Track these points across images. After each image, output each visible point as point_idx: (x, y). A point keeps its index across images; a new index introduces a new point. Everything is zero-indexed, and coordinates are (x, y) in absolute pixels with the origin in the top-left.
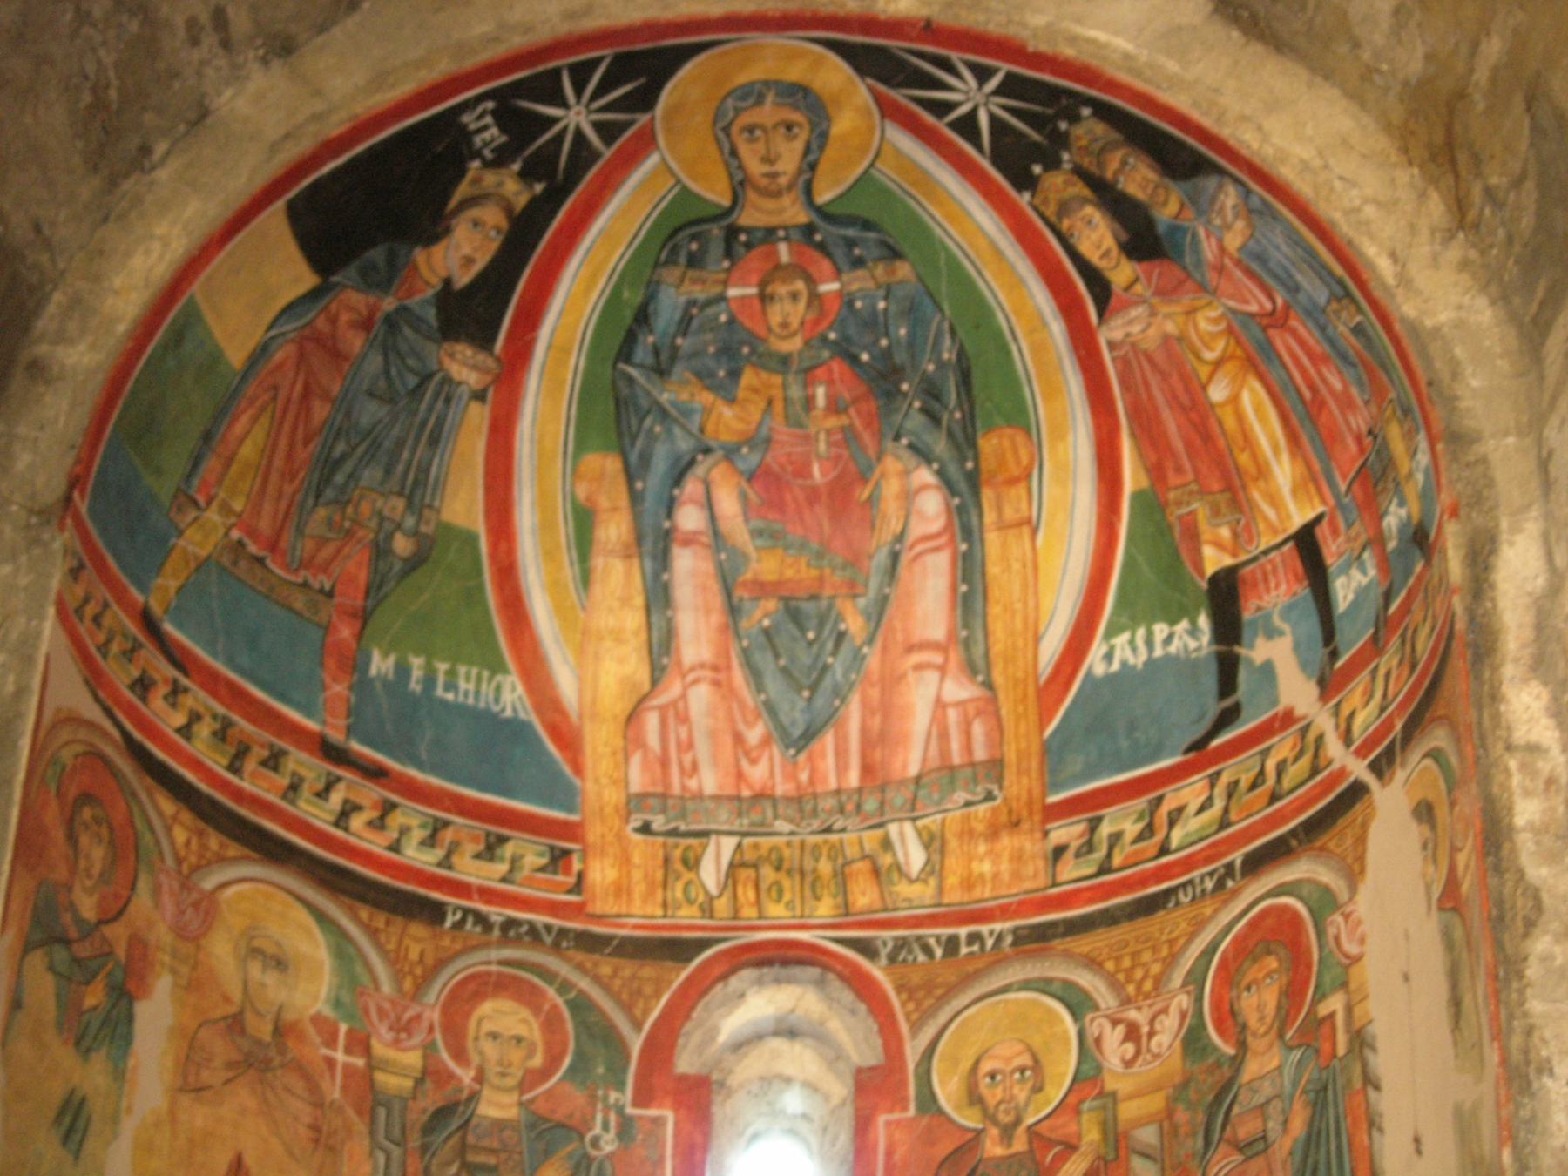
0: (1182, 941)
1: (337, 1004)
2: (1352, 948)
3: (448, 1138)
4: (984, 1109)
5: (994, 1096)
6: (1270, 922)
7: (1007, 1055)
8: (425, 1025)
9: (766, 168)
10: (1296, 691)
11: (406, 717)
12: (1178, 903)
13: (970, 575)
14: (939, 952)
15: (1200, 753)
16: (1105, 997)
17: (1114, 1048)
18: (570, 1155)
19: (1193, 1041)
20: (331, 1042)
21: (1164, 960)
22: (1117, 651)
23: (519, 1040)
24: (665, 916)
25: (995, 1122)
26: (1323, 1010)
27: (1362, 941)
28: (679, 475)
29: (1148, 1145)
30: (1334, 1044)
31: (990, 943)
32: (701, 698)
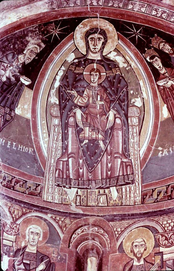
9: (94, 47)
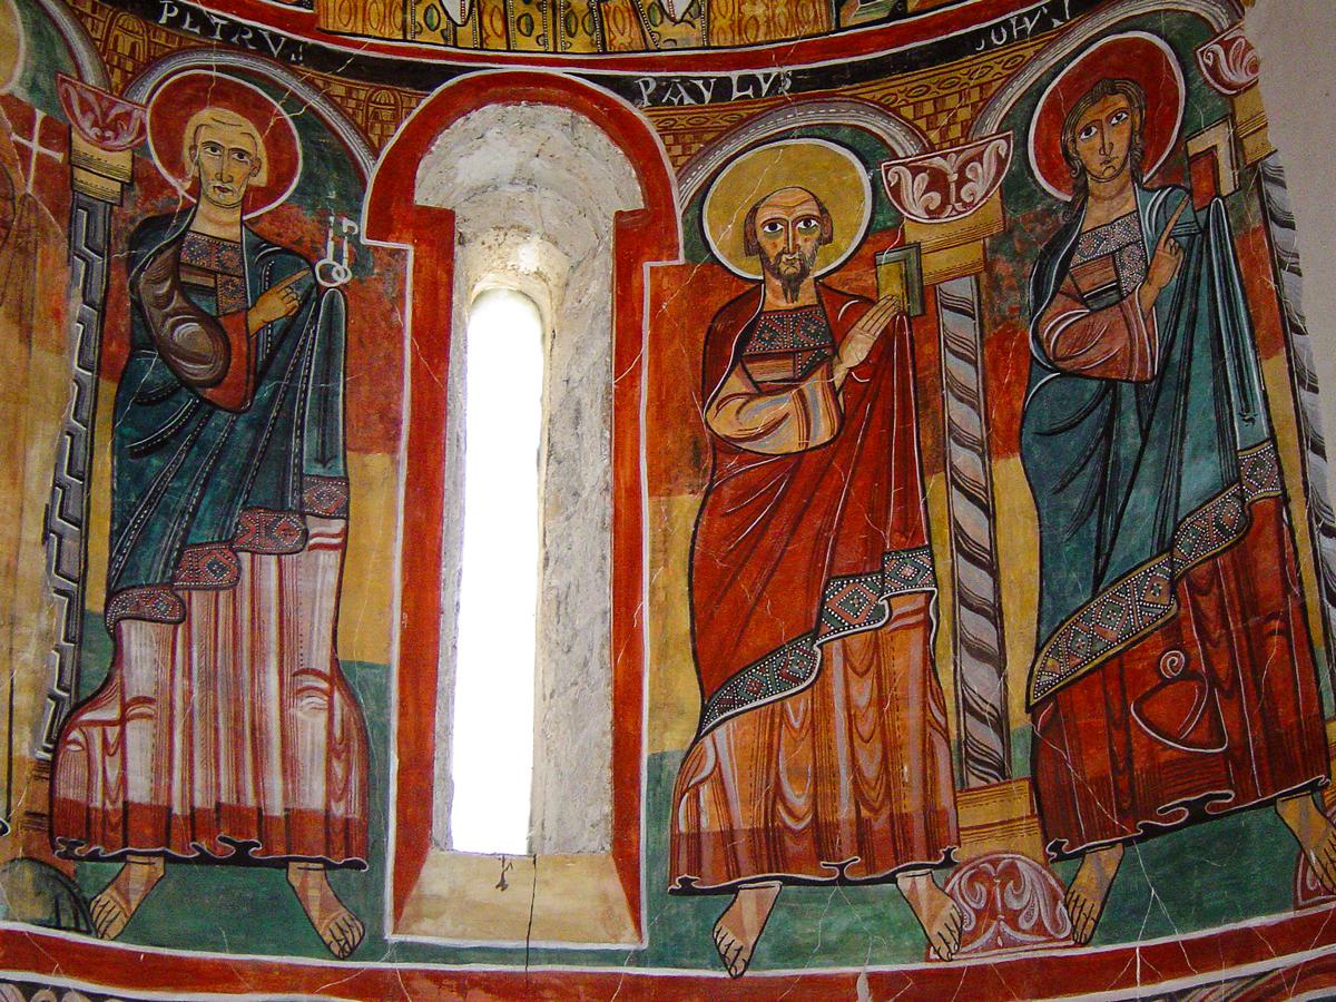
0: (996, 85)
1: (34, 88)
2: (1241, 78)
3: (160, 251)
4: (765, 260)
5: (775, 246)
6: (1113, 59)
7: (789, 203)
8: (135, 124)
12: (989, 46)
14: (708, 96)
16: (904, 145)
17: (916, 197)
18: (298, 284)
19: (1015, 188)
20: (27, 131)
21: (974, 105)
23: (242, 153)
24: (405, 40)
25: (778, 275)
26: (1196, 146)
27: (1254, 68)
29: (964, 300)
30: (1216, 182)
31: (765, 87)
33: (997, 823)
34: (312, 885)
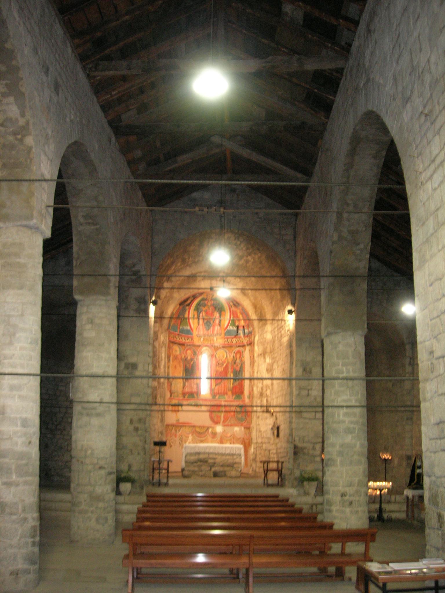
10: (242, 335)
11: (182, 331)
13: (220, 321)
15: (235, 337)
17: (228, 356)
19: (234, 357)
22: (230, 328)
28: (200, 312)
32: (201, 327)
33: (230, 393)
34: (195, 396)
